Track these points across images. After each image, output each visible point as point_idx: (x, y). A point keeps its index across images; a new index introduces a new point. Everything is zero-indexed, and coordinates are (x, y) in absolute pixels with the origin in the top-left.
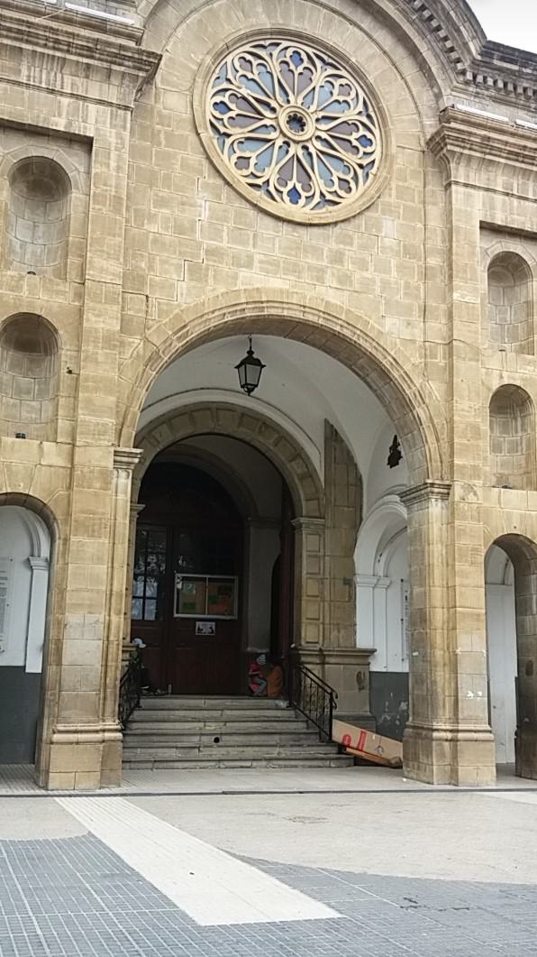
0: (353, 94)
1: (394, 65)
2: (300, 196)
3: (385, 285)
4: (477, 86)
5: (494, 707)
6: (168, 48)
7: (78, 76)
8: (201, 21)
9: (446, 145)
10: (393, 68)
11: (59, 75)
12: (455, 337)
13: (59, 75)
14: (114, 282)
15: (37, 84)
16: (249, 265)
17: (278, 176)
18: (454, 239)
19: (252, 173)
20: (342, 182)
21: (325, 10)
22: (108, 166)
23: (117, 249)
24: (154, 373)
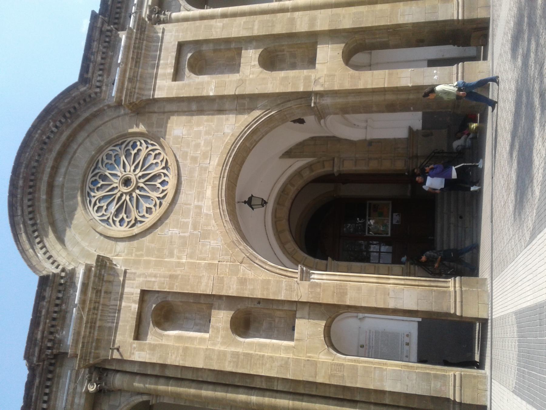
0: (111, 152)
1: (94, 131)
2: (164, 181)
3: (207, 133)
4: (102, 85)
5: (443, 56)
7: (110, 298)
8: (79, 234)
9: (133, 102)
10: (97, 131)
12: (233, 93)
13: (111, 307)
16: (199, 207)
17: (155, 192)
18: (182, 96)
19: (154, 206)
20: (157, 158)
21: (70, 168)
22: (154, 282)
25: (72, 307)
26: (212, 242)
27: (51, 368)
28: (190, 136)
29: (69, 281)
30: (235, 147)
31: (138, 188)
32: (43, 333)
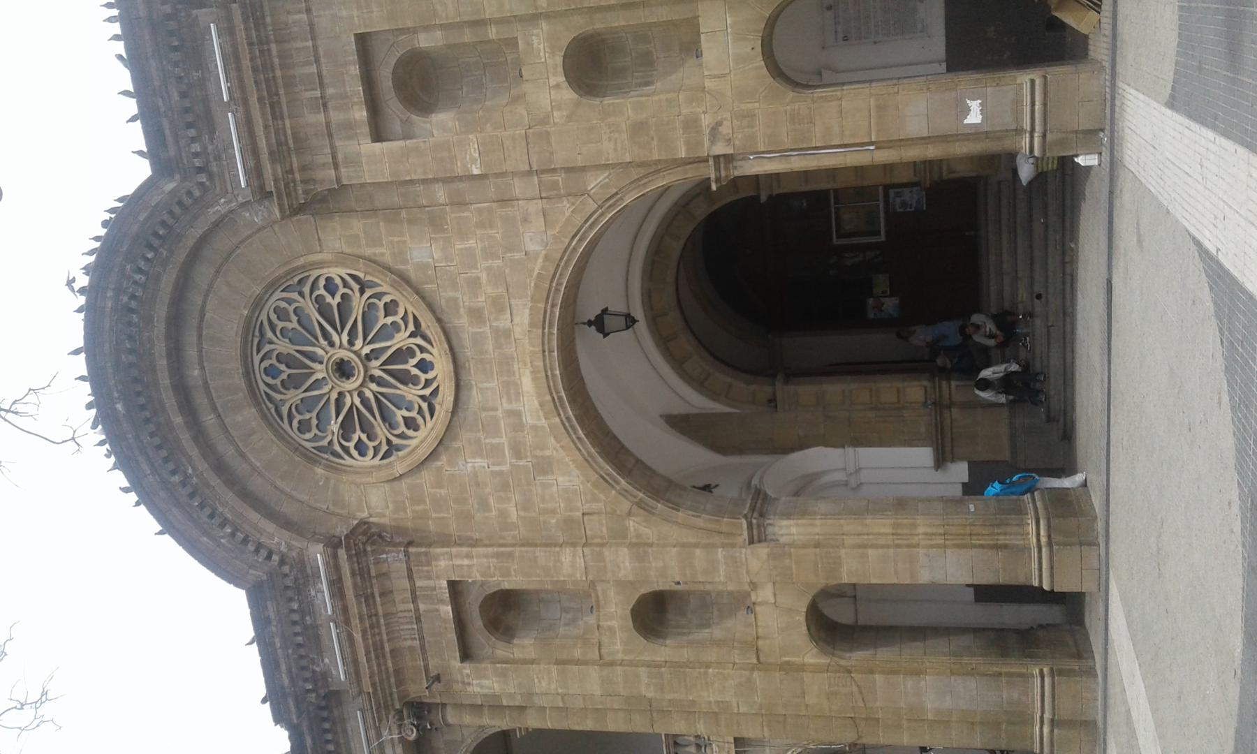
1: (227, 259)
2: (422, 360)
4: (208, 162)
6: (324, 507)
7: (395, 602)
11: (400, 615)
12: (527, 168)
13: (400, 615)
14: (582, 555)
15: (416, 633)
16: (517, 414)
17: (411, 385)
19: (418, 413)
22: (468, 566)
23: (548, 554)
24: (659, 505)
25: (323, 618)
26: (560, 479)
27: (325, 714)
28: (451, 263)
29: (300, 576)
30: (559, 284)
31: (373, 379)
32: (289, 671)
